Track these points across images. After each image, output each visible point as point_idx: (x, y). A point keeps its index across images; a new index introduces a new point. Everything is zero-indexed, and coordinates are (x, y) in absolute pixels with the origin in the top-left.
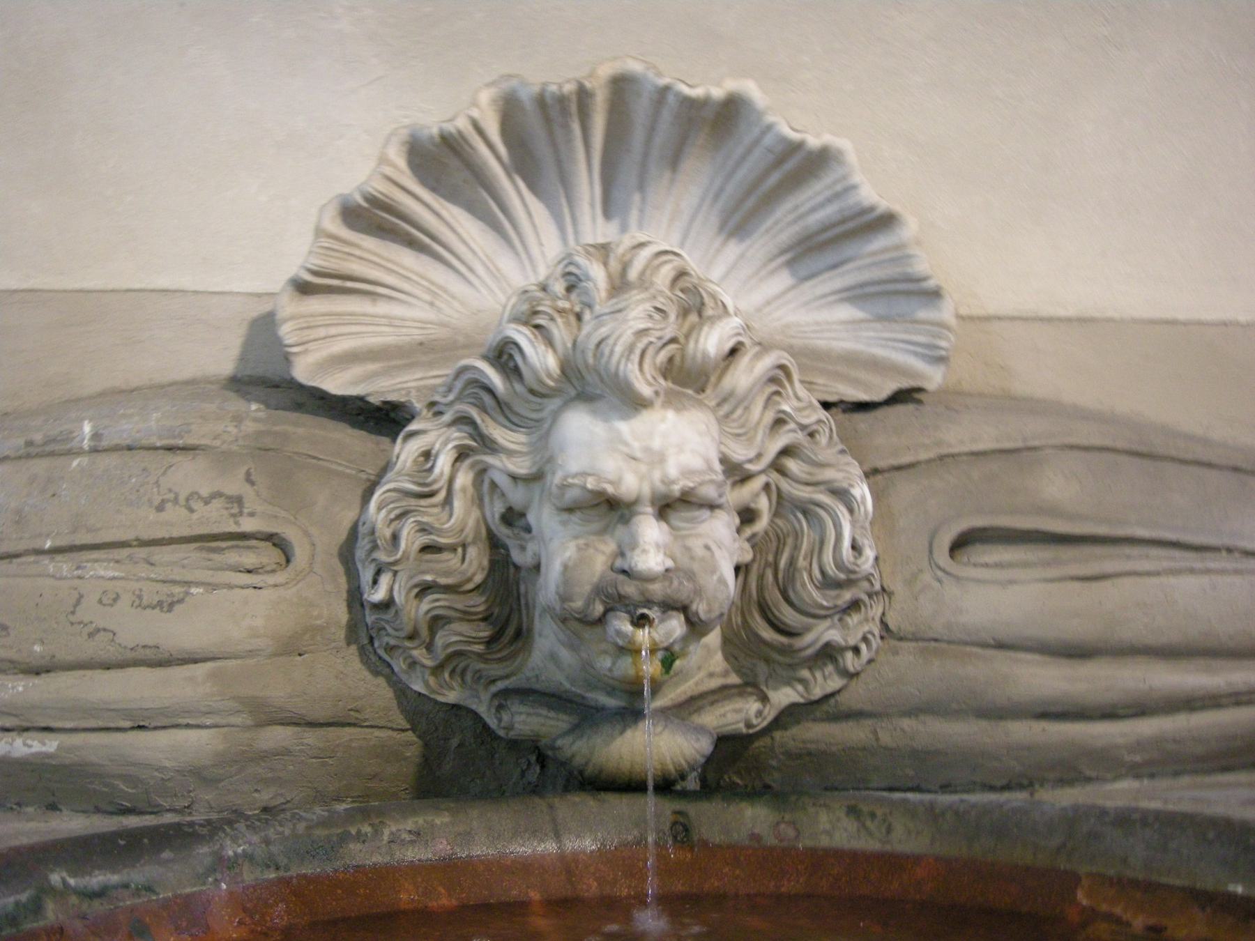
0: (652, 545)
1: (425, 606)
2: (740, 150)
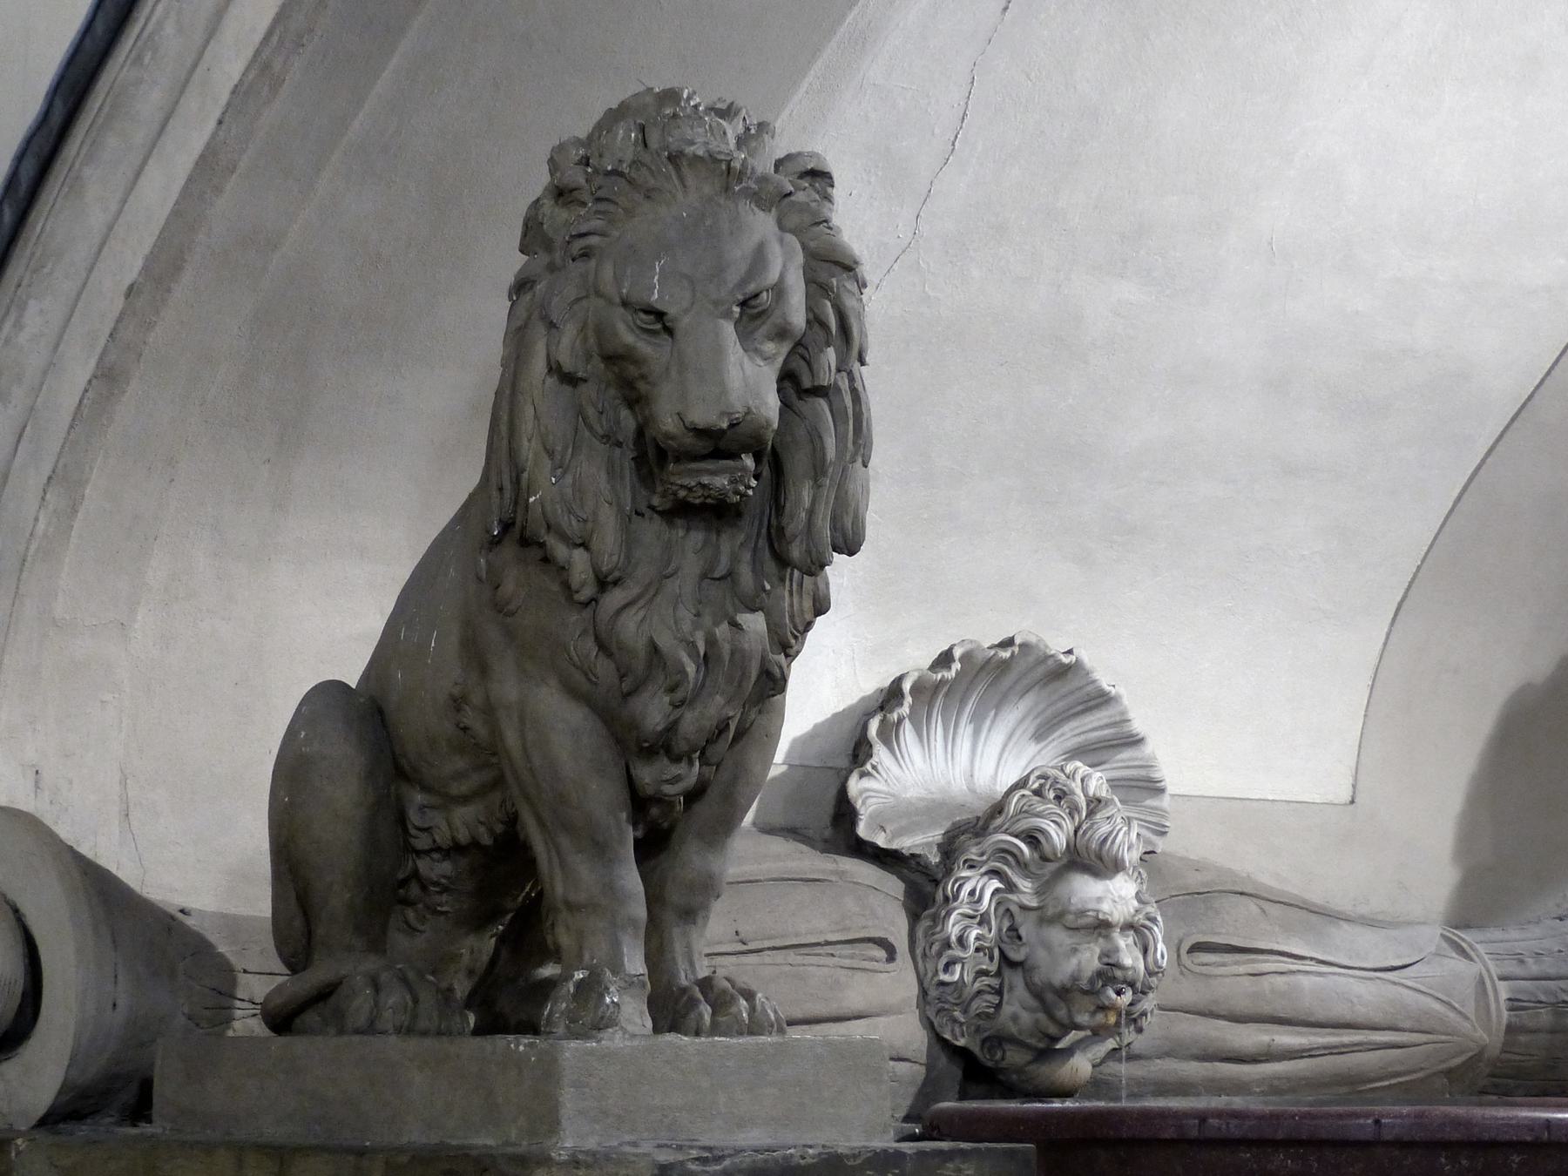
1: (977, 985)
2: (1064, 690)
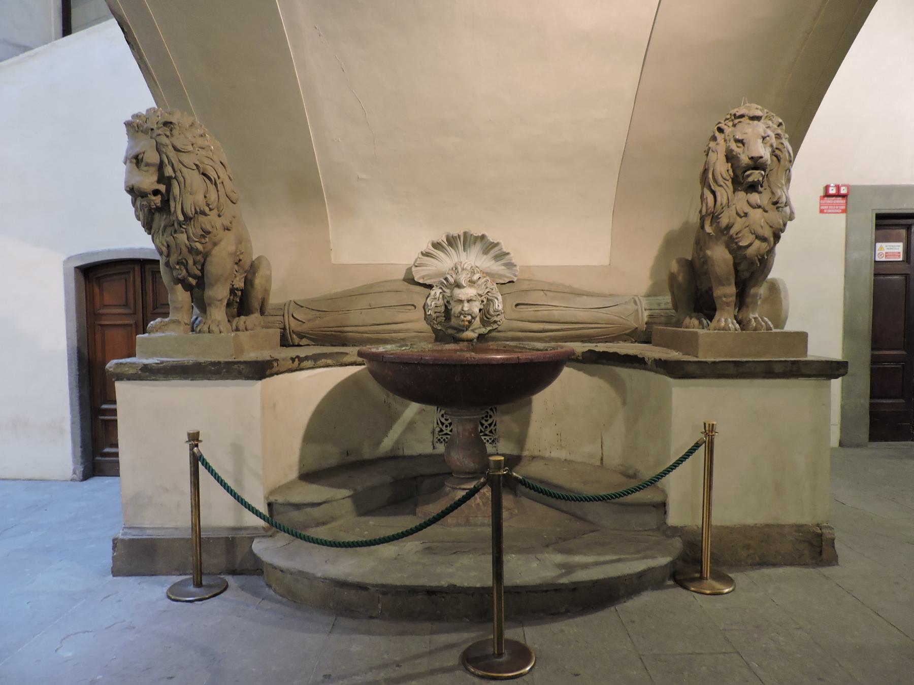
0: (466, 307)
